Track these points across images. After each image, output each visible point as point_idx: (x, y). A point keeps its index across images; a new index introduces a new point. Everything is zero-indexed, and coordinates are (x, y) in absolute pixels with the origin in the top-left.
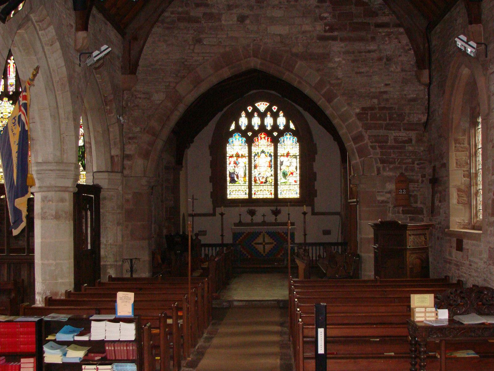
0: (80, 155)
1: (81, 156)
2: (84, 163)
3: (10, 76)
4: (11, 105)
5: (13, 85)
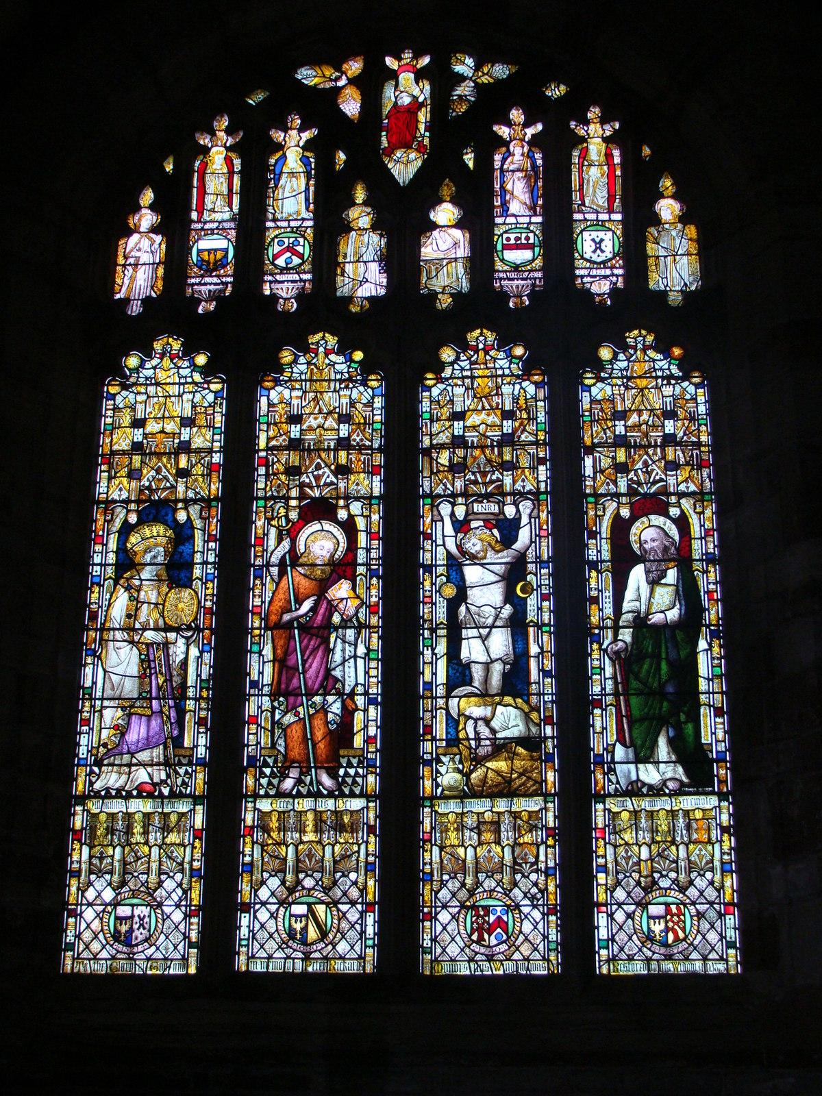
0: (662, 686)
1: (670, 689)
2: (691, 739)
3: (206, 216)
4: (197, 377)
5: (221, 264)
